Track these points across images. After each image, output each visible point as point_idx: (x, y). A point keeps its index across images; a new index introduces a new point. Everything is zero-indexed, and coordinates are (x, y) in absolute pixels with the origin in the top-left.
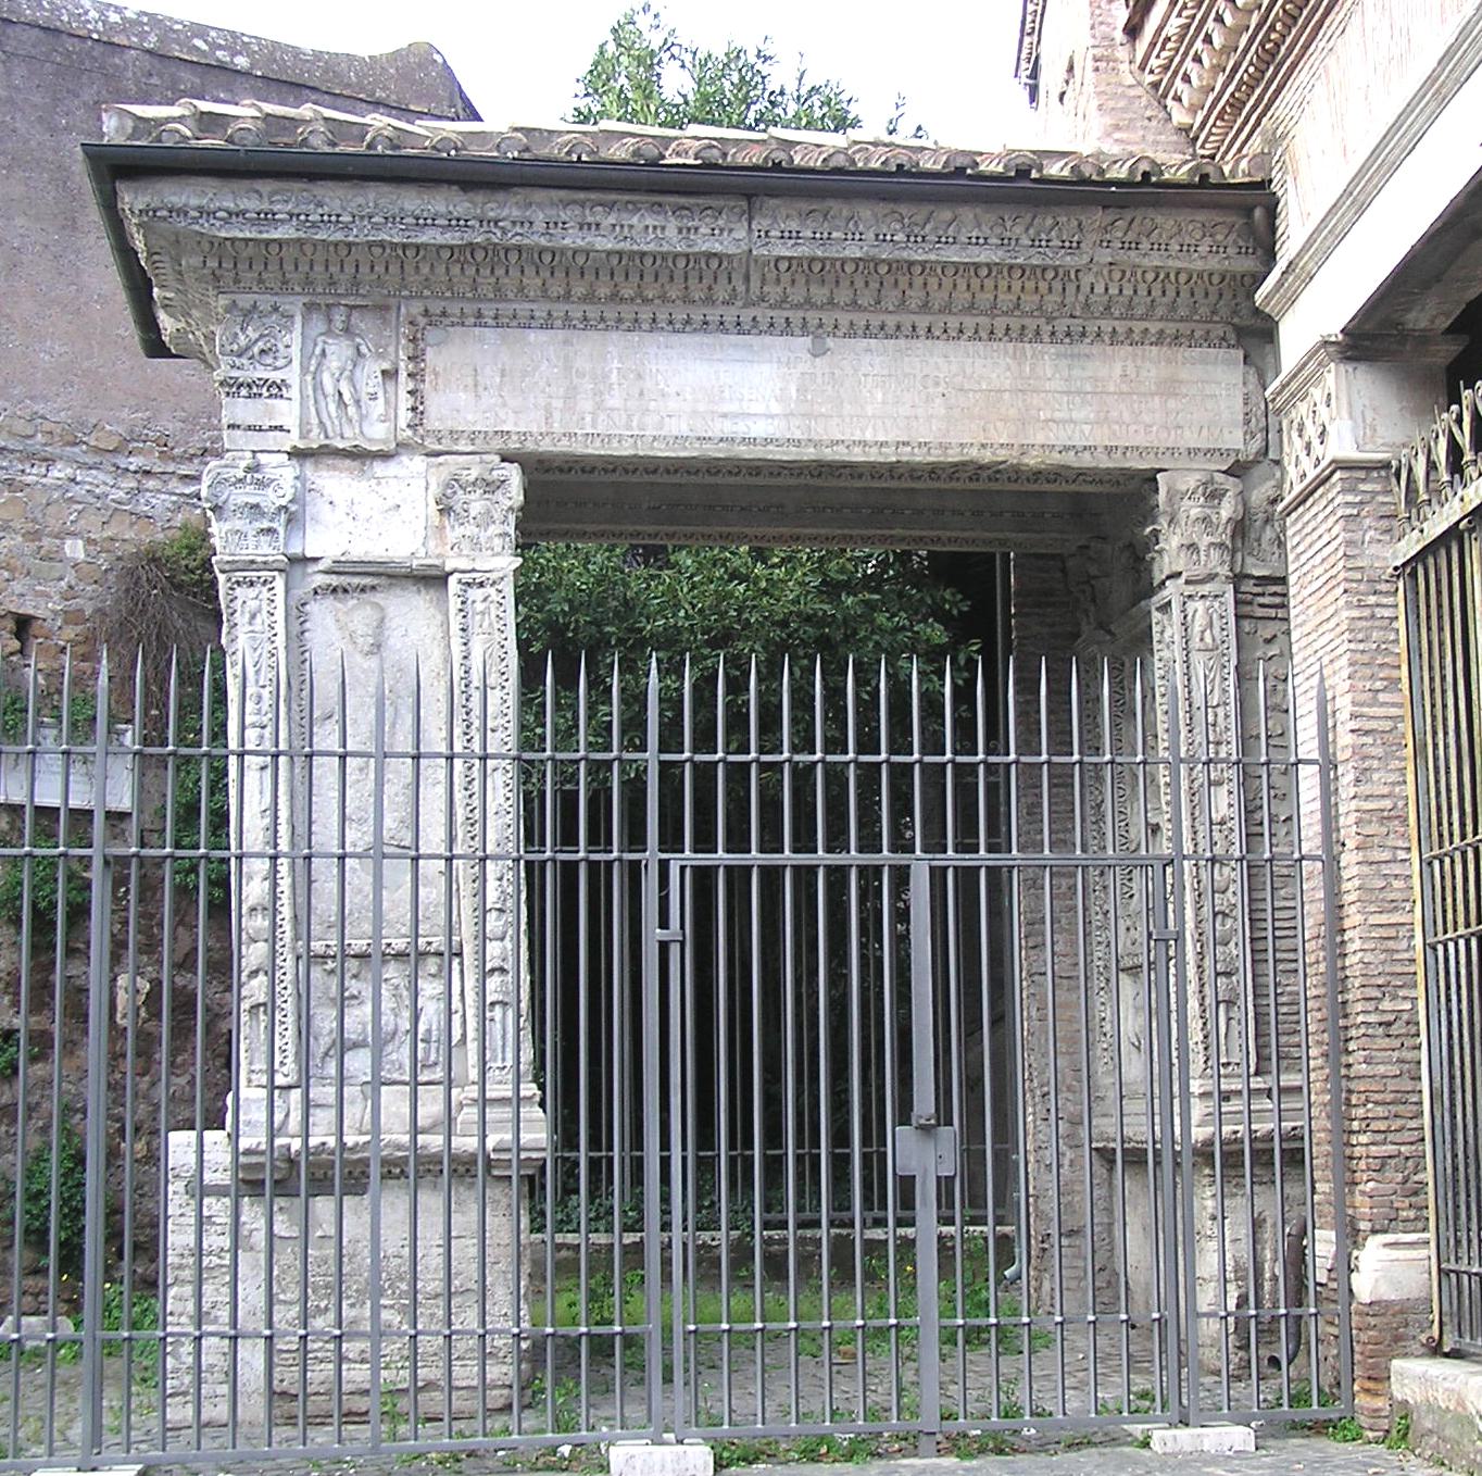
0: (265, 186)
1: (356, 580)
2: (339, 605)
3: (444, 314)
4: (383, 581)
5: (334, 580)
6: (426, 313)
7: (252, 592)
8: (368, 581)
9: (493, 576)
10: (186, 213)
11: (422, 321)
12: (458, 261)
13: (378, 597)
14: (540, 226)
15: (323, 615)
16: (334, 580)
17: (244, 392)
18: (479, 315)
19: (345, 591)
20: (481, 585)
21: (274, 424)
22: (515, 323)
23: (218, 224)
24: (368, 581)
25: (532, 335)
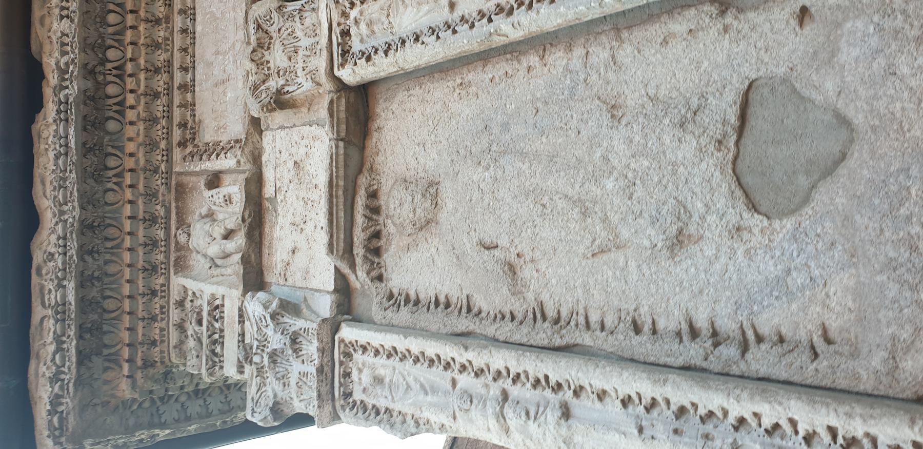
0: (38, 312)
1: (359, 220)
2: (393, 249)
3: (183, 125)
4: (363, 181)
5: (359, 251)
6: (182, 144)
7: (355, 375)
8: (361, 201)
9: (336, 17)
10: (58, 396)
11: (190, 148)
12: (121, 113)
13: (386, 185)
14: (65, 25)
15: (414, 268)
16: (359, 251)
17: (218, 350)
18: (184, 87)
19: (377, 235)
20: (346, 33)
21: (237, 319)
22: (190, 50)
23: (67, 364)
24: (361, 201)
25: (199, 29)
